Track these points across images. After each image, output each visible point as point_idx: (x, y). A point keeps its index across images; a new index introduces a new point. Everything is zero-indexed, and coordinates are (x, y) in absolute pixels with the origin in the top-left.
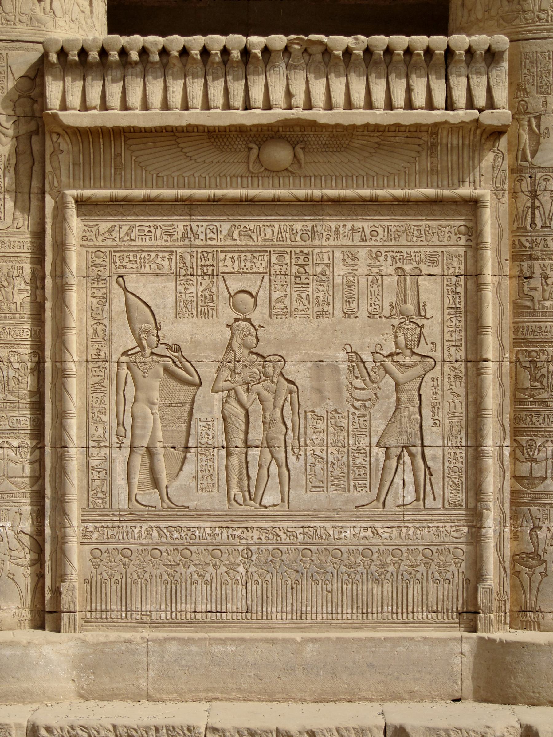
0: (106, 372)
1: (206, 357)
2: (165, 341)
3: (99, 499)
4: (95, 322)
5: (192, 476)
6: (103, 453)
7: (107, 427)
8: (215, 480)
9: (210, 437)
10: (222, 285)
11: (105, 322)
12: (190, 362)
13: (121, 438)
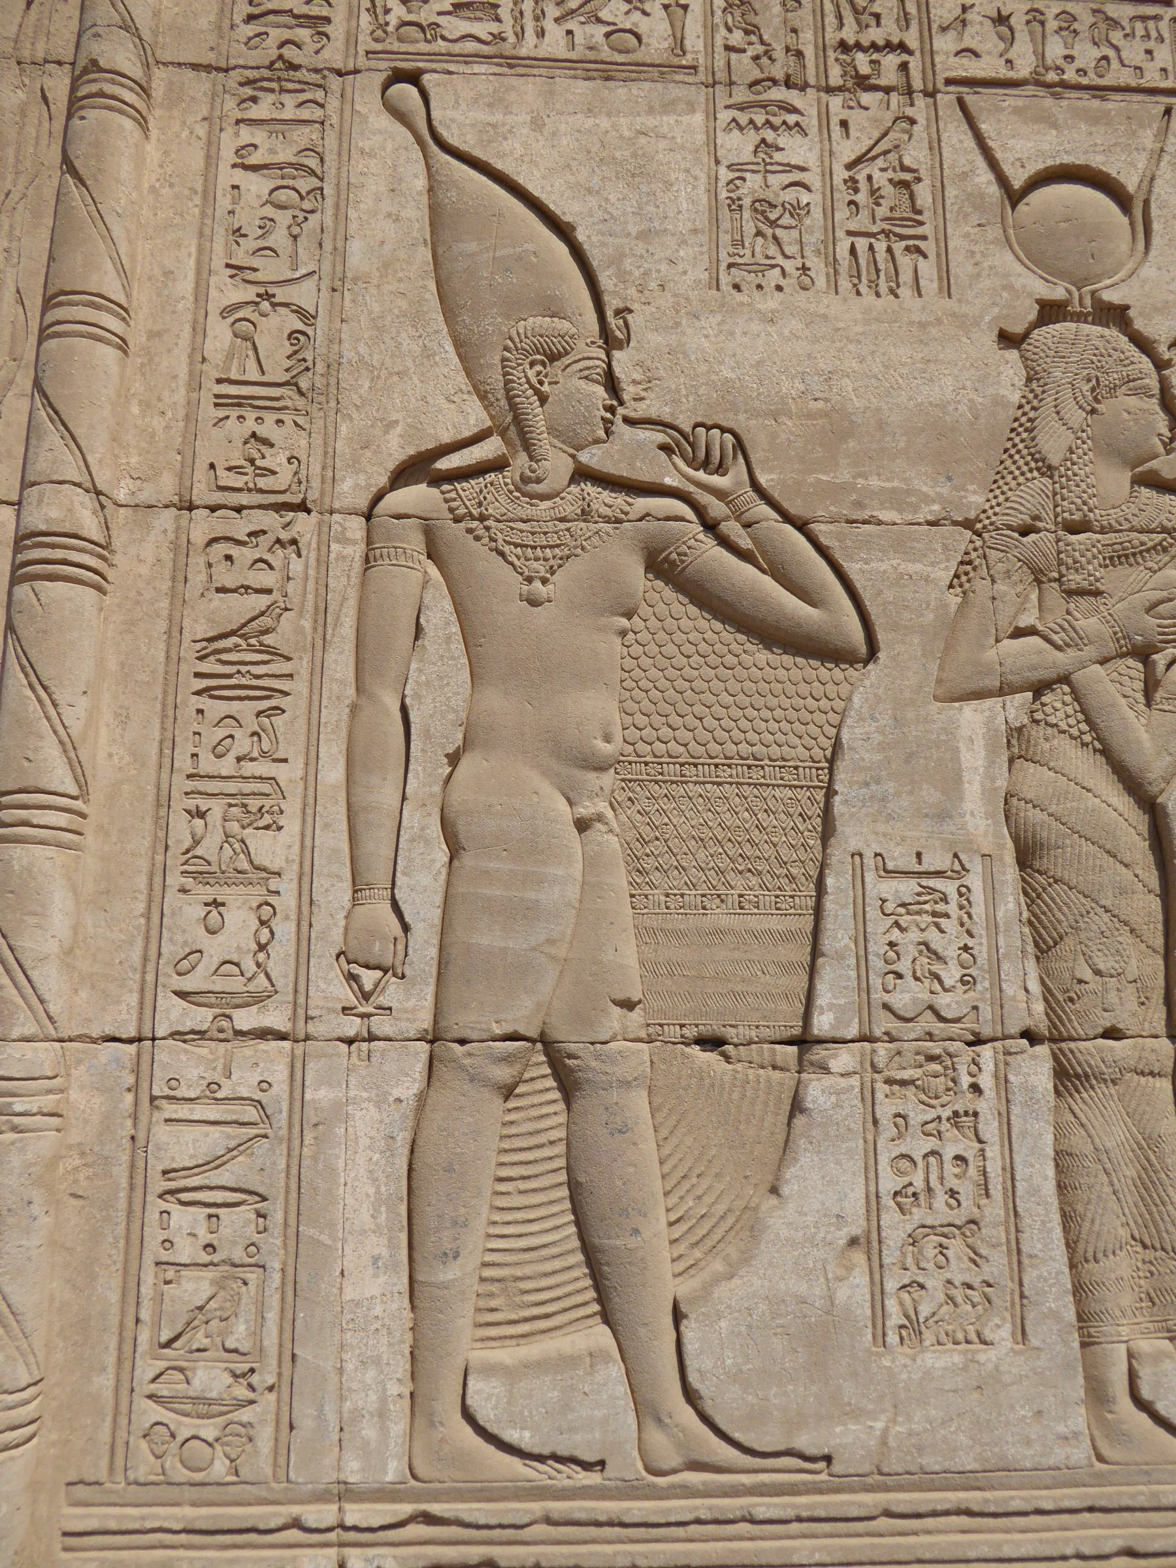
0: (296, 566)
1: (895, 499)
2: (650, 407)
3: (203, 1406)
4: (250, 293)
5: (841, 1237)
6: (244, 1082)
7: (287, 901)
8: (997, 1264)
9: (951, 975)
10: (957, 136)
11: (303, 294)
12: (802, 526)
13: (369, 978)
